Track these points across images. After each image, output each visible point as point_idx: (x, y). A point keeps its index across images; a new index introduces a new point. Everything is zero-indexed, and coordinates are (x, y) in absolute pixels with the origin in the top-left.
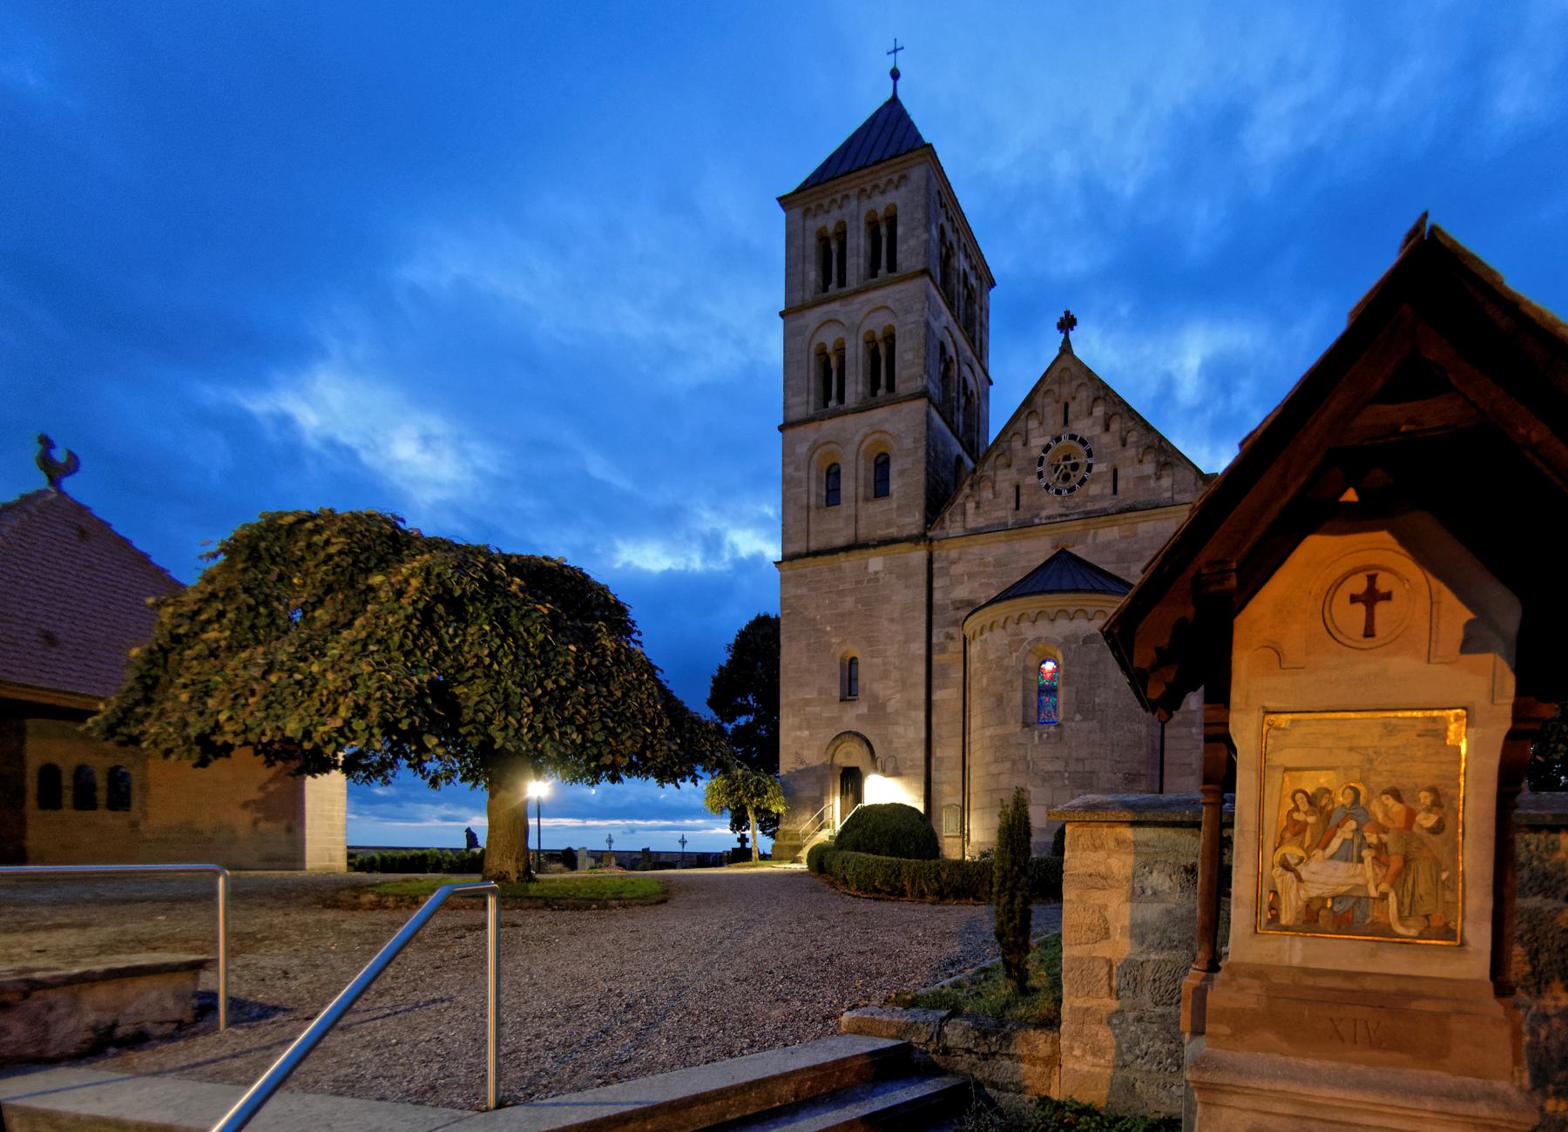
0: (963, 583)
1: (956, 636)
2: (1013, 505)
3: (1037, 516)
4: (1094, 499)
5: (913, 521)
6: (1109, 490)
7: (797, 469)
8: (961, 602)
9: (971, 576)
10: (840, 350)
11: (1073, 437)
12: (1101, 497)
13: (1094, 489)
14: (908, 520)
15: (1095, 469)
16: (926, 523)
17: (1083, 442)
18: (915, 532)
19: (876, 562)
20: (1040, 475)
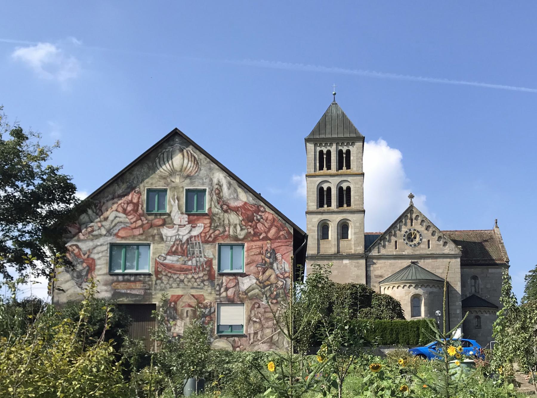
0: (378, 270)
1: (376, 286)
2: (394, 247)
3: (404, 252)
4: (423, 249)
5: (360, 249)
6: (427, 247)
7: (313, 227)
8: (378, 275)
9: (381, 268)
10: (329, 189)
11: (415, 230)
12: (425, 249)
13: (422, 246)
14: (358, 248)
15: (423, 240)
16: (365, 250)
17: (418, 232)
18: (361, 252)
19: (346, 262)
20: (404, 240)
